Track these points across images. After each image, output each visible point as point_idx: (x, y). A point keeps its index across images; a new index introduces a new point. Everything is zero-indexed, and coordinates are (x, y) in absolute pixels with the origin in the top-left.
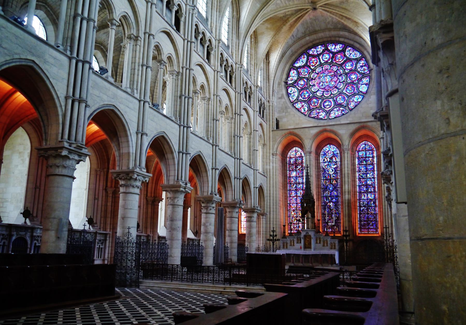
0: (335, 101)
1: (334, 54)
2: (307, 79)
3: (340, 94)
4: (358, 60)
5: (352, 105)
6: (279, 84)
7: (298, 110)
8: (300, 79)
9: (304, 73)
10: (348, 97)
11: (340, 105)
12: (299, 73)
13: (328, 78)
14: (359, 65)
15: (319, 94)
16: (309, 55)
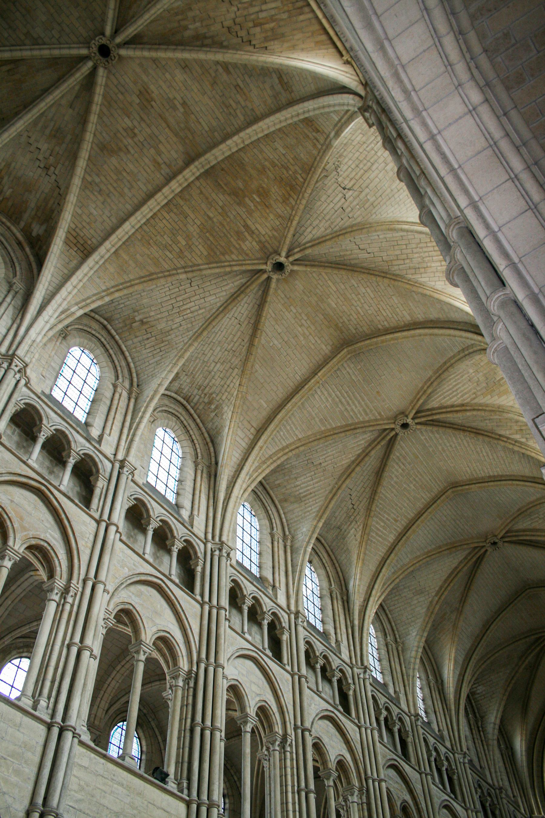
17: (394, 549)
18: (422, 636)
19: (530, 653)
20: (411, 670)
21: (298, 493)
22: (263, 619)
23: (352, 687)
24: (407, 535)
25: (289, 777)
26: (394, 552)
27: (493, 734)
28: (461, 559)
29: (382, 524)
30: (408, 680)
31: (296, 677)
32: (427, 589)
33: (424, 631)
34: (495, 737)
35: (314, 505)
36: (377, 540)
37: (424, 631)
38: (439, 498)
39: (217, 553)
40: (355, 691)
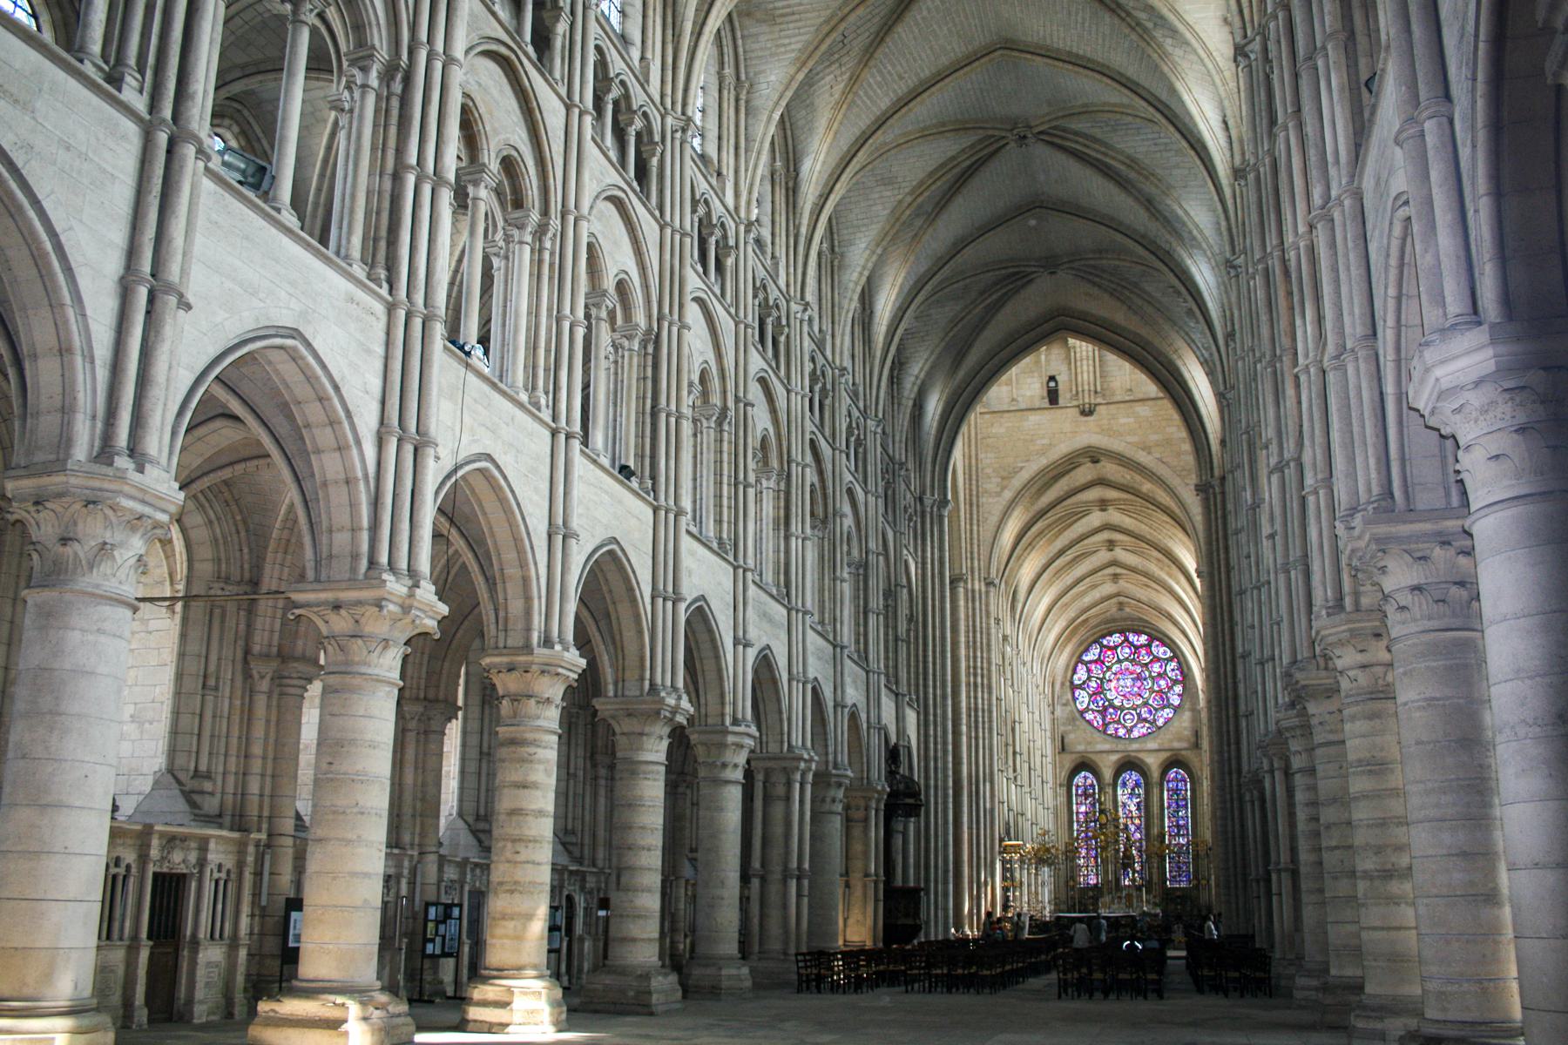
0: (1139, 715)
1: (1137, 648)
2: (1101, 680)
3: (1146, 704)
4: (1170, 659)
5: (1160, 722)
6: (1063, 684)
7: (1089, 722)
8: (1089, 678)
9: (1096, 670)
10: (1156, 710)
11: (1145, 720)
12: (1089, 671)
13: (1129, 683)
14: (1168, 668)
15: (1117, 703)
16: (1102, 646)
17: (884, 123)
18: (874, 252)
19: (997, 291)
20: (847, 301)
21: (771, 6)
22: (712, 234)
23: (786, 330)
24: (911, 105)
25: (725, 466)
26: (884, 128)
27: (911, 391)
28: (964, 145)
29: (879, 79)
30: (840, 315)
31: (742, 326)
32: (899, 180)
33: (878, 245)
34: (913, 396)
35: (795, 36)
36: (863, 102)
37: (878, 245)
38: (977, 59)
39: (678, 135)
40: (788, 337)
